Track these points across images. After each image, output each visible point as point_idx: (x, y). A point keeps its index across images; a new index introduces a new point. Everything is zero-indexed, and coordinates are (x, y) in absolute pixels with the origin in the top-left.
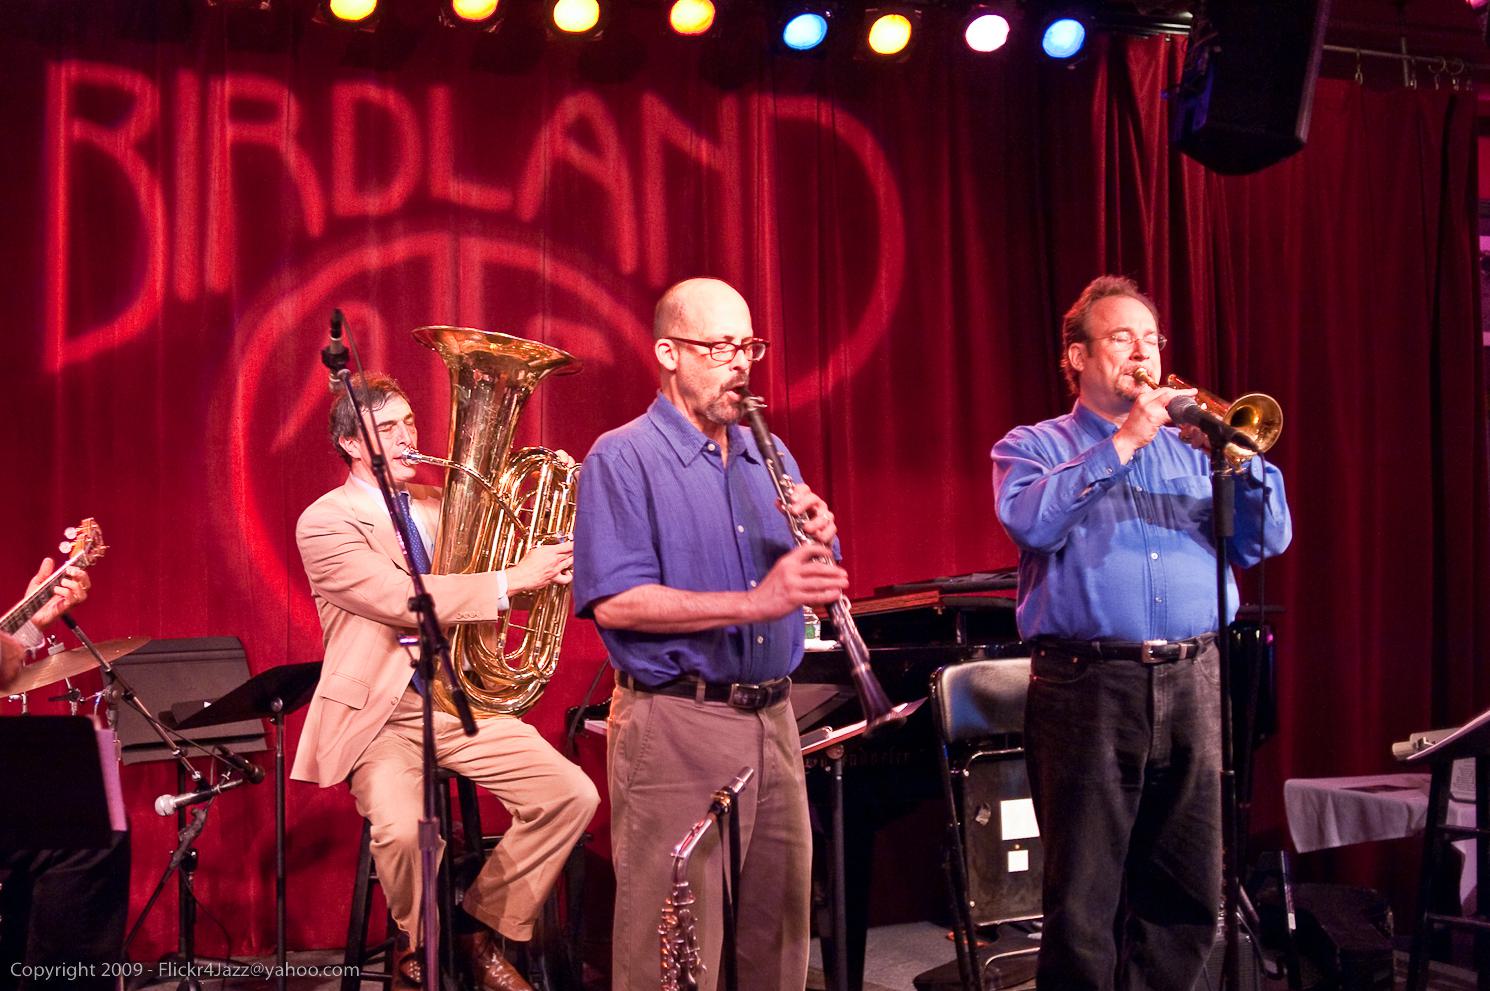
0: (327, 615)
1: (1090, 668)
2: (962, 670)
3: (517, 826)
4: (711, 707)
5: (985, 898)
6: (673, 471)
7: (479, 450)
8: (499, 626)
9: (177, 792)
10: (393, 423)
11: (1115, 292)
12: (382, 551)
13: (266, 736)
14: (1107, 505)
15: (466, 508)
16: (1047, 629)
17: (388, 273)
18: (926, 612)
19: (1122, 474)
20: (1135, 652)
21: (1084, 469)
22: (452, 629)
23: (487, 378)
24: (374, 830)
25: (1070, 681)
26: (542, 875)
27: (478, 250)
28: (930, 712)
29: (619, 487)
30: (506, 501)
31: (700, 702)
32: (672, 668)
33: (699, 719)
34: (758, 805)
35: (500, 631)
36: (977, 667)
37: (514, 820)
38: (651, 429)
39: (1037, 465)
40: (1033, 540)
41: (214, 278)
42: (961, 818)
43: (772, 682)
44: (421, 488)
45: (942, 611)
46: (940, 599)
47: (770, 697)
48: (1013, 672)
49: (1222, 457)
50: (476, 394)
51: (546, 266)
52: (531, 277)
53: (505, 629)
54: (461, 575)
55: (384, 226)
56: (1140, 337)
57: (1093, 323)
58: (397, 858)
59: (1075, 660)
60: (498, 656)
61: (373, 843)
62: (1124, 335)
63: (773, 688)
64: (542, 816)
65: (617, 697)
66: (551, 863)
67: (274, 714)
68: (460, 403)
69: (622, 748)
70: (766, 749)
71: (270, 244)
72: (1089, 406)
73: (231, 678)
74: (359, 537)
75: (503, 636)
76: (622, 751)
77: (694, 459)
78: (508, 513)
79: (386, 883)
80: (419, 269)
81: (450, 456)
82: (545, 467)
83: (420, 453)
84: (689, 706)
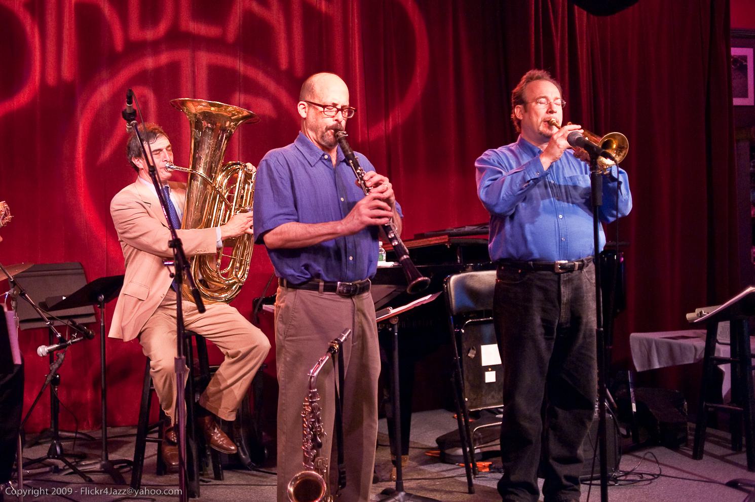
0: (127, 251)
1: (527, 275)
2: (460, 277)
3: (227, 360)
4: (327, 295)
5: (473, 396)
6: (305, 169)
7: (205, 164)
8: (217, 256)
9: (48, 345)
10: (160, 150)
11: (538, 78)
12: (155, 217)
13: (95, 314)
14: (536, 192)
15: (199, 194)
16: (505, 256)
17: (158, 70)
18: (441, 247)
19: (544, 175)
20: (551, 267)
21: (524, 173)
22: (192, 258)
23: (209, 125)
24: (152, 363)
25: (516, 282)
26: (241, 386)
27: (205, 58)
28: (444, 298)
30: (220, 190)
31: (321, 293)
32: (306, 274)
33: (321, 302)
34: (352, 347)
35: (217, 258)
36: (468, 275)
37: (226, 357)
39: (499, 170)
40: (497, 210)
41: (67, 72)
42: (460, 354)
44: (175, 183)
45: (450, 246)
46: (449, 239)
47: (358, 289)
48: (487, 277)
49: (596, 164)
50: (204, 134)
51: (240, 66)
52: (233, 72)
53: (220, 257)
54: (197, 230)
55: (155, 47)
56: (552, 101)
57: (527, 95)
58: (164, 378)
59: (520, 271)
60: (217, 272)
61: (151, 370)
62: (543, 100)
64: (240, 355)
65: (279, 292)
66: (246, 380)
67: (100, 303)
68: (195, 139)
70: (356, 317)
71: (96, 55)
72: (526, 139)
73: (76, 284)
74: (144, 210)
75: (219, 261)
77: (317, 163)
78: (221, 196)
79: (159, 391)
80: (174, 68)
81: (191, 167)
82: (240, 172)
83: (175, 165)
84: (315, 295)
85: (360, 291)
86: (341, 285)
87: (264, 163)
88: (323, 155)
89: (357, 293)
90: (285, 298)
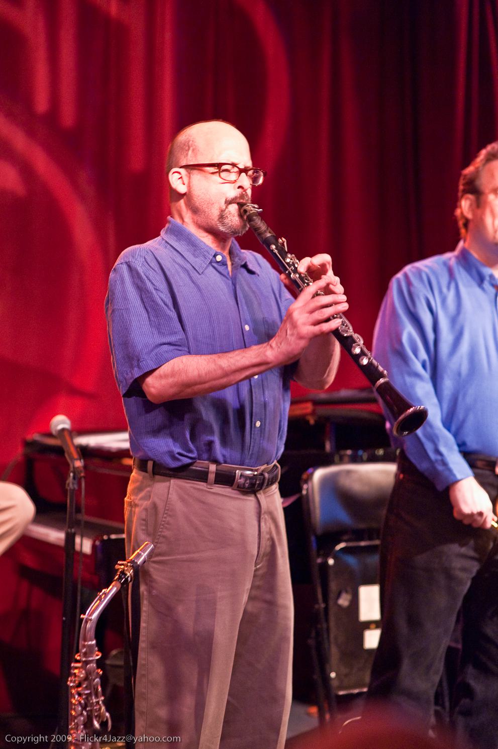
4: (218, 489)
6: (191, 278)
31: (211, 485)
32: (190, 451)
43: (265, 466)
63: (268, 473)
65: (135, 481)
69: (142, 525)
70: (263, 524)
76: (144, 528)
86: (242, 475)
87: (125, 267)
88: (215, 256)
89: (264, 488)
90: (150, 492)
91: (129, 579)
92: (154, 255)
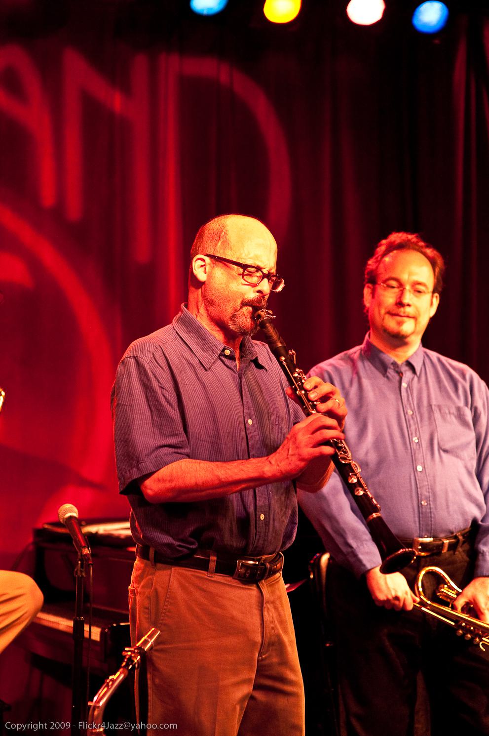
6: (196, 374)
29: (155, 384)
38: (176, 338)
70: (265, 613)
85: (269, 573)
87: (132, 361)
91: (136, 665)
92: (163, 352)
